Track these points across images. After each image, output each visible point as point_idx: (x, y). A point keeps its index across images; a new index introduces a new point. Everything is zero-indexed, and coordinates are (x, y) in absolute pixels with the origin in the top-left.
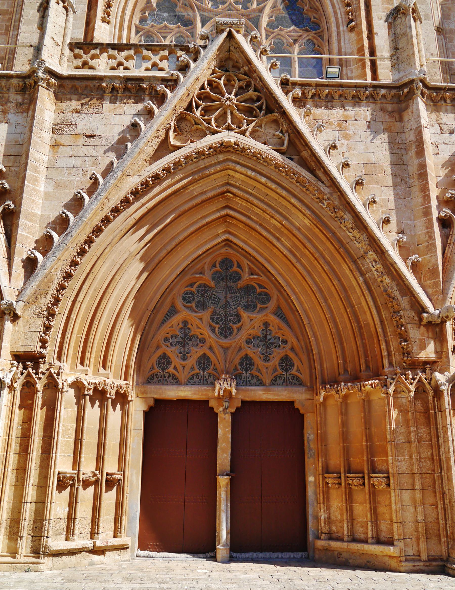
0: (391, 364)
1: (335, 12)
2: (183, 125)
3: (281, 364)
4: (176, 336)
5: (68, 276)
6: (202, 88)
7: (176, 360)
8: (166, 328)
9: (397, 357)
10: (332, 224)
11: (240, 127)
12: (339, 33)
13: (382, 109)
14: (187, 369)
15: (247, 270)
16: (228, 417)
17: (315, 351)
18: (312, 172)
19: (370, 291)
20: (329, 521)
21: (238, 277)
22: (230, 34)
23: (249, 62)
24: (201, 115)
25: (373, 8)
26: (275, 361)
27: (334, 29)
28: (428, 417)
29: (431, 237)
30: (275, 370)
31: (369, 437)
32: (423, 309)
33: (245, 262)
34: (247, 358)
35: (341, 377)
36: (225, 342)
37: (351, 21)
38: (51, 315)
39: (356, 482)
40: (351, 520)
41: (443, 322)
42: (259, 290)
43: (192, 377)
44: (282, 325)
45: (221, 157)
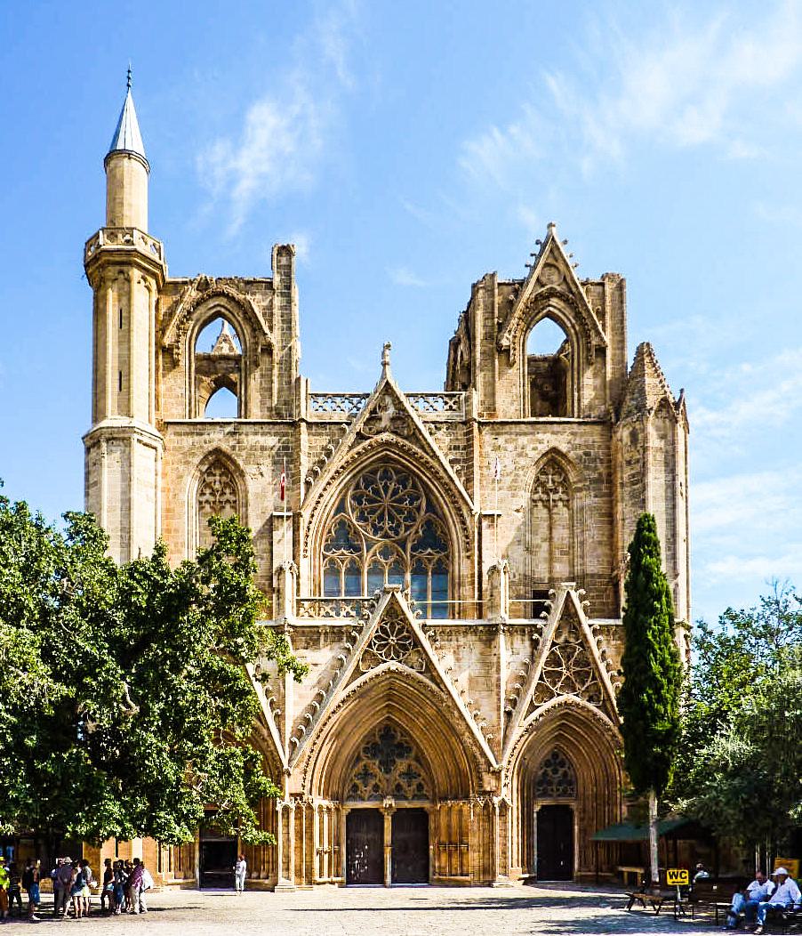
0: (473, 792)
1: (458, 538)
2: (366, 655)
4: (360, 774)
5: (312, 751)
6: (377, 632)
11: (398, 657)
15: (399, 734)
16: (390, 818)
18: (438, 685)
20: (440, 867)
21: (393, 737)
24: (377, 650)
25: (483, 539)
26: (414, 786)
27: (457, 554)
30: (414, 791)
31: (460, 827)
32: (490, 765)
33: (398, 729)
34: (399, 787)
36: (387, 776)
37: (468, 551)
38: (305, 772)
42: (405, 745)
44: (419, 766)
45: (388, 676)
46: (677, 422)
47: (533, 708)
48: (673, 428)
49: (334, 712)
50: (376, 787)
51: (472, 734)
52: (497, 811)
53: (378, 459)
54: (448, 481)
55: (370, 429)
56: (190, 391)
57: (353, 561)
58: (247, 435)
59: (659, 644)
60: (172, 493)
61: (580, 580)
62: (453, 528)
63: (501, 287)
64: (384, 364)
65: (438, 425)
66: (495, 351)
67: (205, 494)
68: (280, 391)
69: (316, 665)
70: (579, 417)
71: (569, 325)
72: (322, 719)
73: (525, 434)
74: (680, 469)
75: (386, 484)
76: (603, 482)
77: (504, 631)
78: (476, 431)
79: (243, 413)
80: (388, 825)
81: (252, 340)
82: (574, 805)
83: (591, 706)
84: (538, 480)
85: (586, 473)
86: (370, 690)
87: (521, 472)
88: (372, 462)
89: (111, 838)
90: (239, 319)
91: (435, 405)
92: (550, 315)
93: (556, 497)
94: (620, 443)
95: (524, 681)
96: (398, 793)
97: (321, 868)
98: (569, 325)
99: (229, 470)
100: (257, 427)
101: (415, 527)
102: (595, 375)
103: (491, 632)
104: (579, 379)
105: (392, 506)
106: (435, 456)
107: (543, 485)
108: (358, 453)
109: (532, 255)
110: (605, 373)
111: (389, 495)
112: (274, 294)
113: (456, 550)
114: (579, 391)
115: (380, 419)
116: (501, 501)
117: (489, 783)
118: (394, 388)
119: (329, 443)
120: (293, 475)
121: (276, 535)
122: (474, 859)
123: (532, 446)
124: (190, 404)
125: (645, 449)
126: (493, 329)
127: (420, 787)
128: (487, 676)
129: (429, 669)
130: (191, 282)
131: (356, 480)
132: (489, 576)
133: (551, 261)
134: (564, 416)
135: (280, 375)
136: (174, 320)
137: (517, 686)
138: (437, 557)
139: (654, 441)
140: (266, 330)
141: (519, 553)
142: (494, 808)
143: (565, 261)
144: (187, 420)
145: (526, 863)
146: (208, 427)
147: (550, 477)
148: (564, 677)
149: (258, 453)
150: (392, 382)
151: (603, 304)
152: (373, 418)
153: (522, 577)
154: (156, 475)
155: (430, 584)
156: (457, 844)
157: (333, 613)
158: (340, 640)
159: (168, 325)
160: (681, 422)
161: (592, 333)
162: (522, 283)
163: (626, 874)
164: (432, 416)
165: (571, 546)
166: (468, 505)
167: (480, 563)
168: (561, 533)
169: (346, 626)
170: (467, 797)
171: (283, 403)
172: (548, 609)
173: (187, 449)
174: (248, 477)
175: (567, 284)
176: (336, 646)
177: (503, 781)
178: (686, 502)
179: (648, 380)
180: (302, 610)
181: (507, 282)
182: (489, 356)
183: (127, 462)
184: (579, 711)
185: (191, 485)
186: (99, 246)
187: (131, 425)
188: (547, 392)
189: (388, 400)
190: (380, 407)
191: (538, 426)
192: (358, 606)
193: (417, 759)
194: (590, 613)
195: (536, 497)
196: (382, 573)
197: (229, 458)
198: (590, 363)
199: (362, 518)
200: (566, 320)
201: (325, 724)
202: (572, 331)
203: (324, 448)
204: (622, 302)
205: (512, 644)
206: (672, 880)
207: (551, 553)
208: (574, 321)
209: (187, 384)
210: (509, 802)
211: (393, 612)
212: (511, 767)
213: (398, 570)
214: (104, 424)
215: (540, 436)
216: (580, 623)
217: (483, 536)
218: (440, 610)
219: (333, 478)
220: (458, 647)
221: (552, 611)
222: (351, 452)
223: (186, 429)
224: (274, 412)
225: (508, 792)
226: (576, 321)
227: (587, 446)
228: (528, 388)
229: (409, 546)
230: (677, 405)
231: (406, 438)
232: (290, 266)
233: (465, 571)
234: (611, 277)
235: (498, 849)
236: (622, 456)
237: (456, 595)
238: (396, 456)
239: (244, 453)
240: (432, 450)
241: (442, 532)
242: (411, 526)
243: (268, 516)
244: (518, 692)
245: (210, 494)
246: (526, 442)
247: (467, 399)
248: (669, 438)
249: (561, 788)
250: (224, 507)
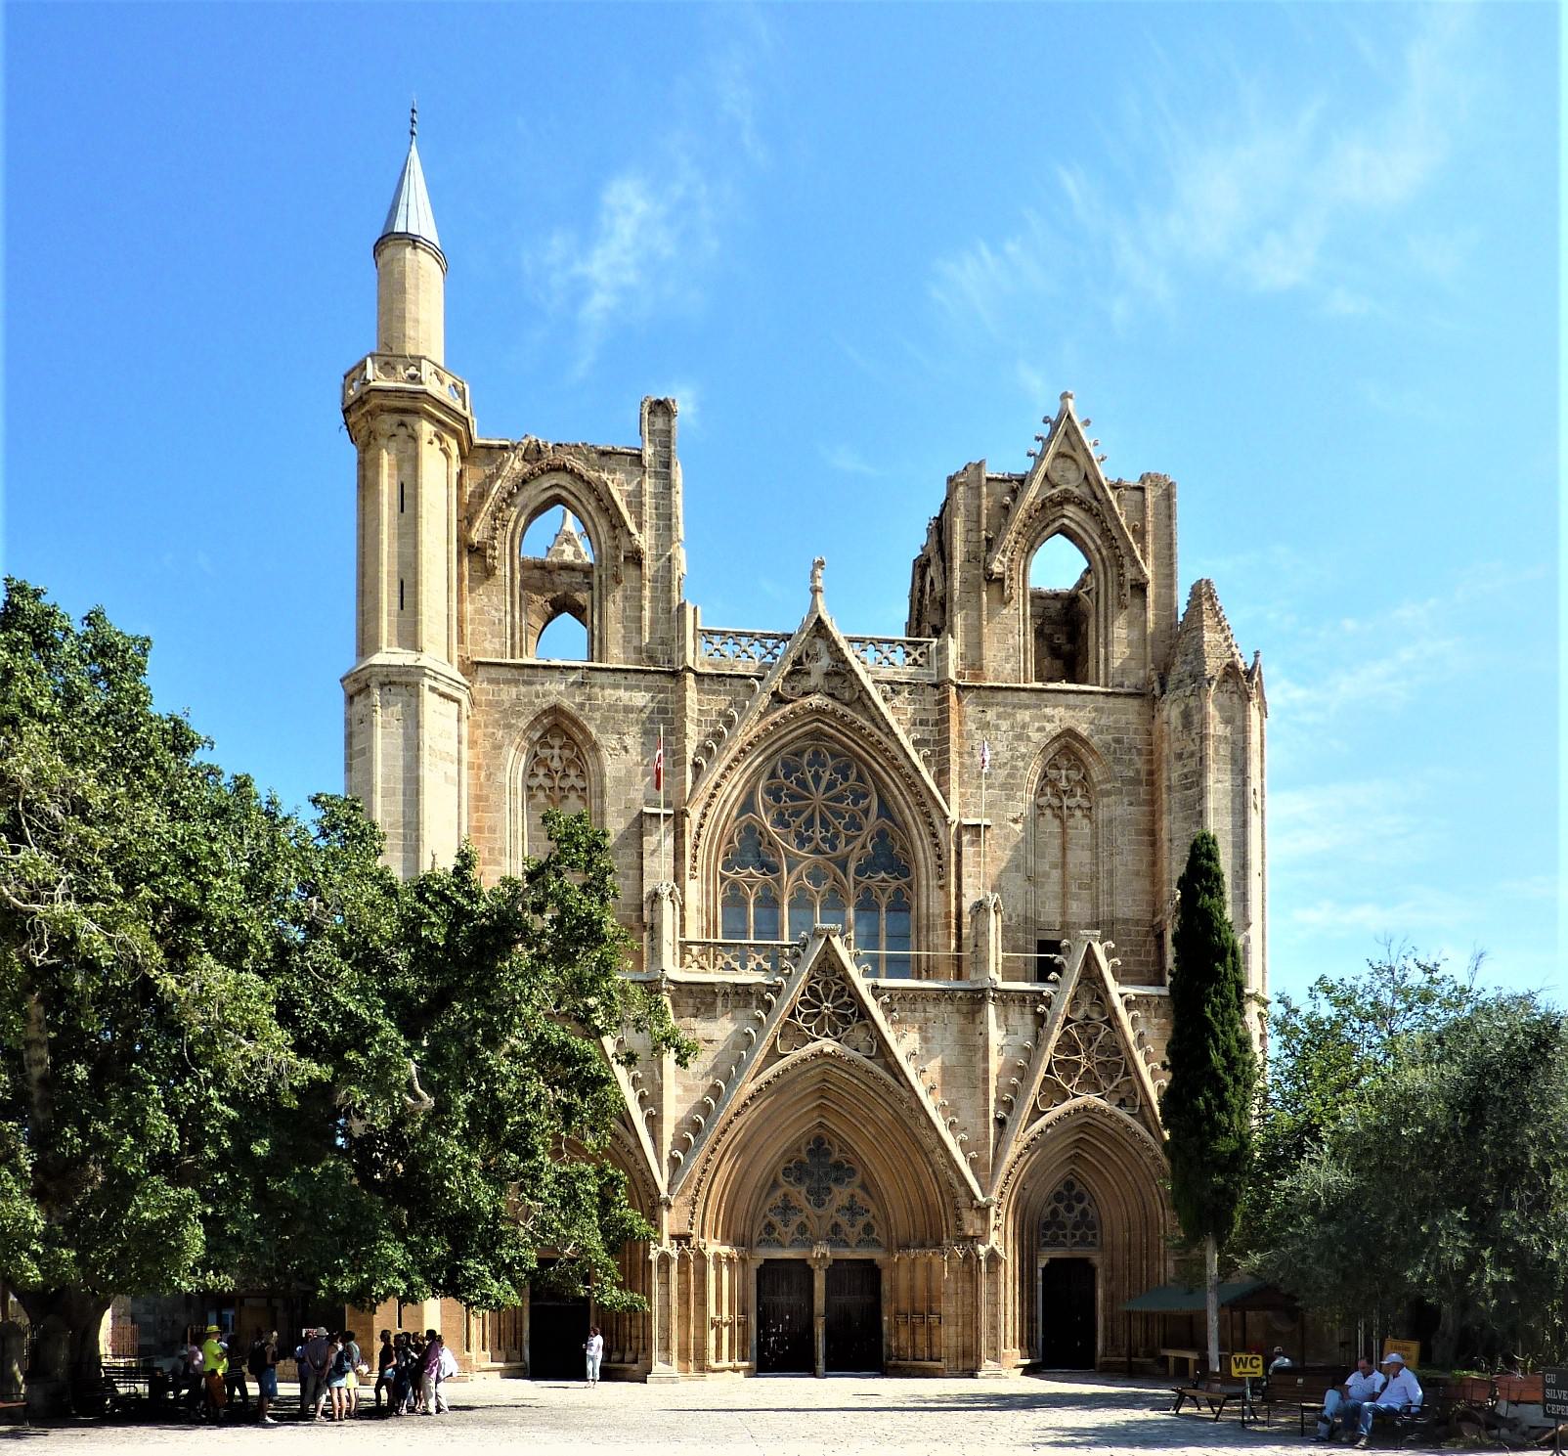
0: (948, 1236)
1: (926, 859)
2: (787, 1029)
3: (864, 1229)
6: (803, 994)
7: (780, 1227)
8: (771, 1201)
9: (953, 1232)
10: (911, 1123)
12: (928, 885)
13: (958, 1011)
14: (790, 1234)
16: (823, 1273)
17: (892, 1221)
19: (936, 1178)
20: (898, 1348)
21: (828, 1153)
22: (828, 939)
23: (845, 969)
25: (964, 861)
26: (859, 1227)
27: (924, 883)
28: (971, 1275)
29: (987, 1136)
31: (929, 1290)
32: (975, 1198)
34: (836, 1225)
35: (912, 1244)
36: (819, 1212)
39: (918, 1320)
40: (914, 1347)
41: (989, 1207)
43: (793, 1241)
44: (866, 1197)
45: (820, 1061)
46: (1249, 699)
47: (1037, 1114)
48: (1245, 710)
49: (737, 1114)
50: (802, 1228)
51: (946, 1150)
52: (984, 1265)
53: (806, 734)
54: (911, 772)
55: (793, 688)
56: (513, 617)
57: (766, 887)
58: (602, 688)
59: (1222, 1024)
60: (486, 772)
61: (1107, 927)
62: (919, 843)
63: (992, 483)
64: (815, 591)
65: (895, 687)
66: (982, 579)
67: (537, 776)
68: (653, 622)
69: (710, 1041)
70: (1106, 686)
71: (1092, 547)
72: (720, 1123)
73: (1027, 707)
74: (1254, 770)
75: (816, 772)
76: (1140, 783)
77: (994, 999)
78: (953, 698)
79: (596, 653)
80: (819, 1283)
81: (609, 544)
82: (1097, 1259)
83: (1123, 1114)
84: (1046, 776)
85: (1117, 768)
86: (793, 1081)
87: (1021, 764)
88: (798, 738)
89: (391, 1298)
90: (590, 508)
91: (891, 656)
92: (1064, 531)
93: (1072, 802)
94: (1165, 726)
95: (1024, 1073)
96: (835, 1236)
97: (719, 1347)
98: (1092, 547)
99: (573, 740)
100: (619, 676)
101: (860, 840)
102: (1130, 624)
103: (976, 999)
104: (1106, 627)
105: (825, 806)
106: (891, 733)
107: (1053, 783)
108: (775, 724)
109: (1038, 439)
110: (1145, 622)
111: (822, 789)
112: (644, 472)
113: (923, 876)
114: (1106, 647)
115: (808, 674)
116: (990, 805)
117: (972, 1225)
118: (829, 627)
119: (730, 706)
120: (674, 753)
121: (649, 842)
122: (949, 1336)
123: (1037, 725)
124: (513, 635)
125: (1203, 738)
126: (979, 547)
127: (868, 1228)
128: (970, 1064)
129: (883, 1050)
130: (515, 448)
131: (773, 763)
132: (973, 917)
133: (1066, 449)
134: (1084, 681)
135: (653, 599)
136: (487, 505)
137: (1014, 1080)
138: (894, 884)
139: (1216, 727)
140: (633, 529)
141: (1017, 883)
142: (979, 1261)
143: (1086, 450)
144: (509, 661)
145: (1027, 1343)
146: (541, 672)
147: (1063, 772)
148: (1082, 1070)
149: (620, 716)
150: (826, 618)
151: (1143, 518)
152: (798, 670)
153: (1021, 918)
154: (460, 742)
155: (883, 924)
156: (923, 1314)
157: (736, 965)
158: (747, 1005)
159: (477, 512)
160: (1256, 701)
161: (1127, 561)
162: (1022, 481)
163: (1171, 1361)
164: (887, 673)
165: (1095, 877)
166: (941, 808)
167: (959, 896)
168: (1079, 858)
169: (756, 984)
170: (939, 1244)
171: (659, 641)
172: (1059, 969)
173: (507, 705)
174: (604, 753)
175: (1090, 485)
176: (740, 1014)
177: (993, 1222)
178: (1263, 818)
179: (1208, 636)
180: (688, 958)
181: (1000, 477)
182: (971, 587)
183: (413, 722)
184: (1106, 1121)
185: (514, 763)
187: (419, 664)
188: (1060, 645)
189: (820, 645)
190: (808, 655)
191: (1045, 695)
192: (774, 956)
193: (864, 1187)
194: (1121, 975)
195: (1042, 801)
196: (813, 906)
197: (575, 722)
198: (1123, 606)
199: (781, 821)
200: (1088, 541)
201: (724, 1132)
202: (1098, 556)
203: (720, 714)
204: (1170, 517)
205: (1006, 1017)
206: (1238, 1370)
207: (1064, 884)
208: (1099, 542)
209: (508, 604)
210: (1001, 1252)
211: (829, 964)
212: (1004, 1201)
213: (834, 903)
214: (377, 659)
215: (1048, 711)
216: (1106, 991)
217: (963, 855)
218: (898, 967)
219: (736, 760)
220: (927, 1020)
221: (1066, 972)
222: (763, 723)
223: (508, 674)
224: (644, 655)
225: (999, 1238)
226: (1103, 542)
227: (1118, 729)
228: (1031, 637)
229: (852, 867)
230: (1249, 674)
231: (847, 705)
232: (670, 432)
233: (936, 908)
234: (1156, 479)
235: (984, 1319)
236: (1170, 746)
237: (924, 944)
238: (832, 731)
239: (597, 715)
240: (888, 724)
241: (902, 848)
242: (856, 837)
243: (636, 813)
244: (1014, 1090)
245: (545, 775)
246: (1028, 719)
247: (942, 650)
248: (1239, 723)
249: (1078, 1233)
250: (566, 797)
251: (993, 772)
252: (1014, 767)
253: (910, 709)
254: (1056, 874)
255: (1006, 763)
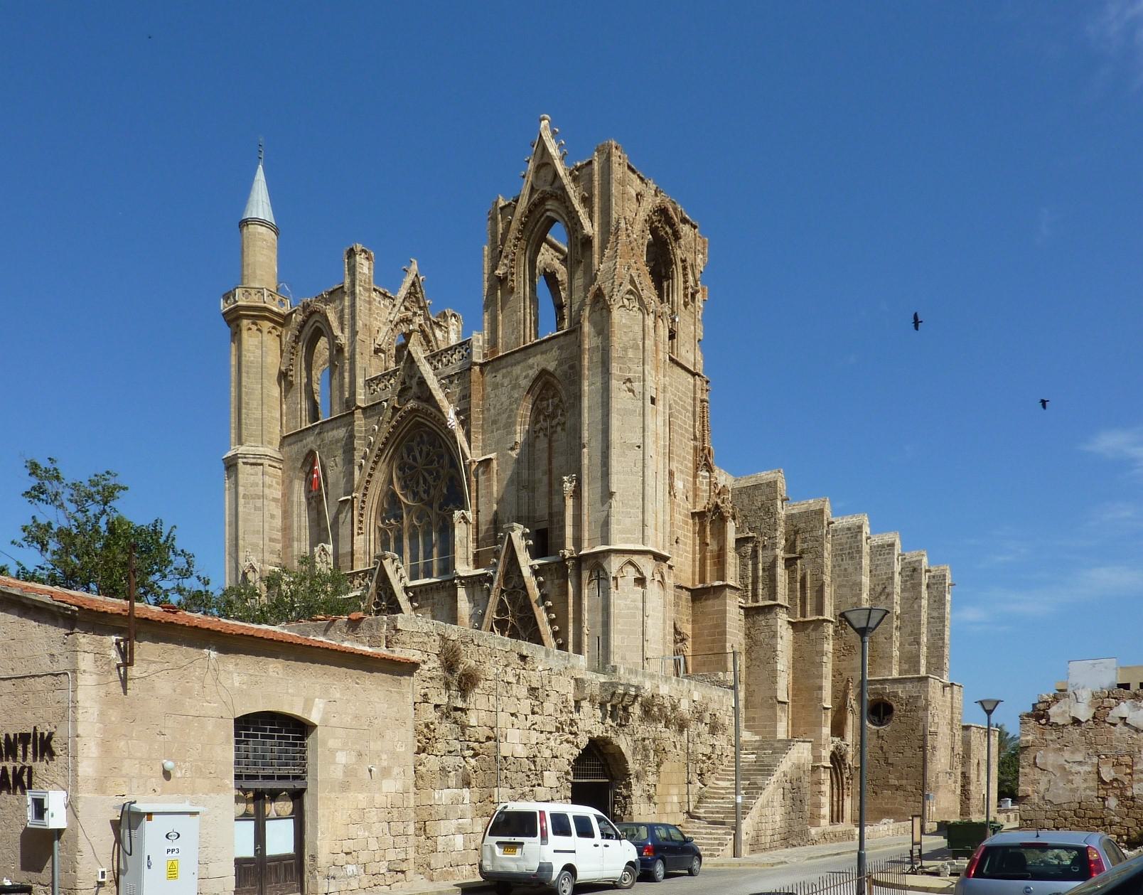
58: (328, 432)
186: (236, 302)
215: (531, 361)
229: (436, 506)
231: (425, 401)
246: (519, 372)
251: (500, 418)
252: (511, 410)
253: (458, 390)
254: (545, 478)
255: (507, 409)
